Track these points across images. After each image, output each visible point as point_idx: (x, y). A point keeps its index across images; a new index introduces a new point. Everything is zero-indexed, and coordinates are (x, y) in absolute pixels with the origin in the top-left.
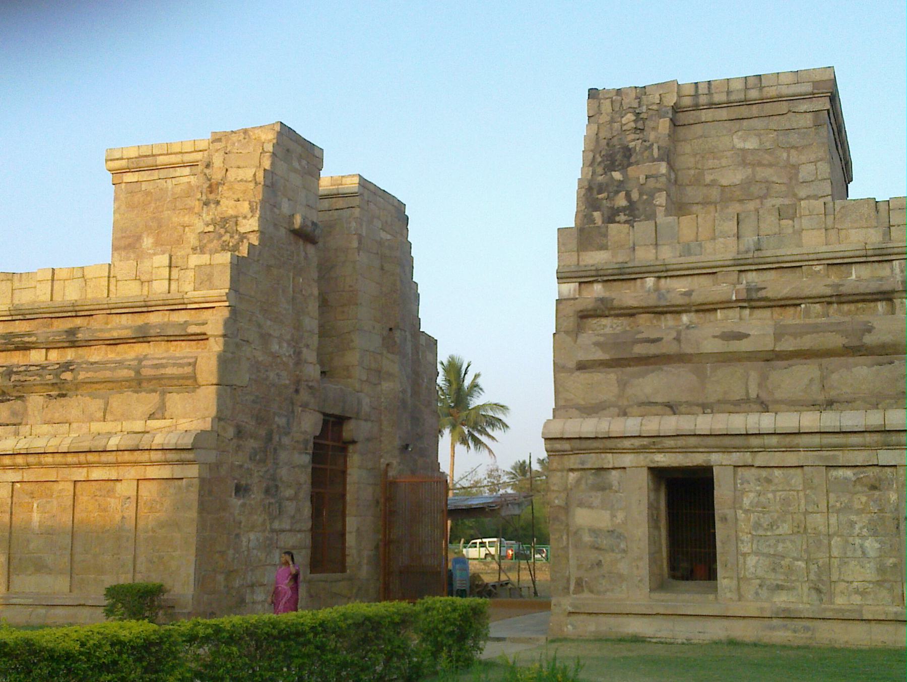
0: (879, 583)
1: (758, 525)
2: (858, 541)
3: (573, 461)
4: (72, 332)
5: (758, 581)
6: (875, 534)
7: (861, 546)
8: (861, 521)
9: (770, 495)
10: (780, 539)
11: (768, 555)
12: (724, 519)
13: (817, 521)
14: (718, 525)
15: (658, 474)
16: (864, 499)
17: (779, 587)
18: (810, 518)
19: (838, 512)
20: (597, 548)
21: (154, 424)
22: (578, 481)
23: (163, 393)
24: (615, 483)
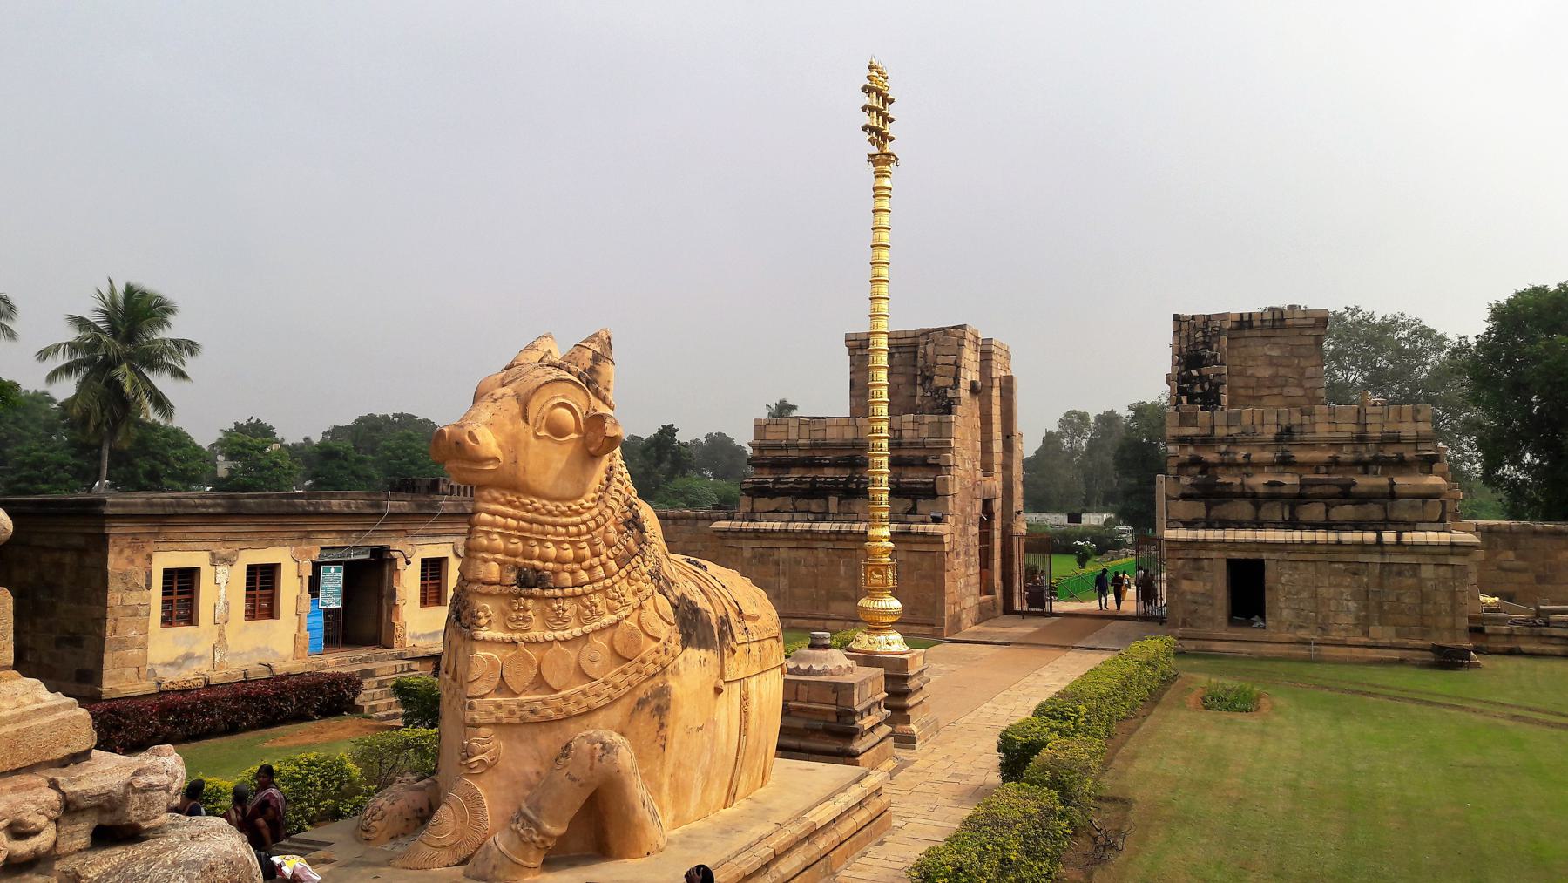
0: (1355, 625)
1: (1290, 593)
2: (1345, 602)
3: (1181, 554)
4: (853, 457)
5: (1288, 623)
6: (1354, 599)
7: (1347, 605)
8: (1347, 593)
9: (1297, 576)
10: (1301, 601)
11: (1295, 609)
12: (1270, 589)
13: (1323, 591)
14: (1267, 592)
15: (1232, 564)
16: (1349, 580)
17: (1301, 627)
18: (1319, 590)
19: (1335, 586)
20: (1196, 603)
21: (911, 517)
22: (1184, 565)
23: (915, 500)
24: (1206, 566)
